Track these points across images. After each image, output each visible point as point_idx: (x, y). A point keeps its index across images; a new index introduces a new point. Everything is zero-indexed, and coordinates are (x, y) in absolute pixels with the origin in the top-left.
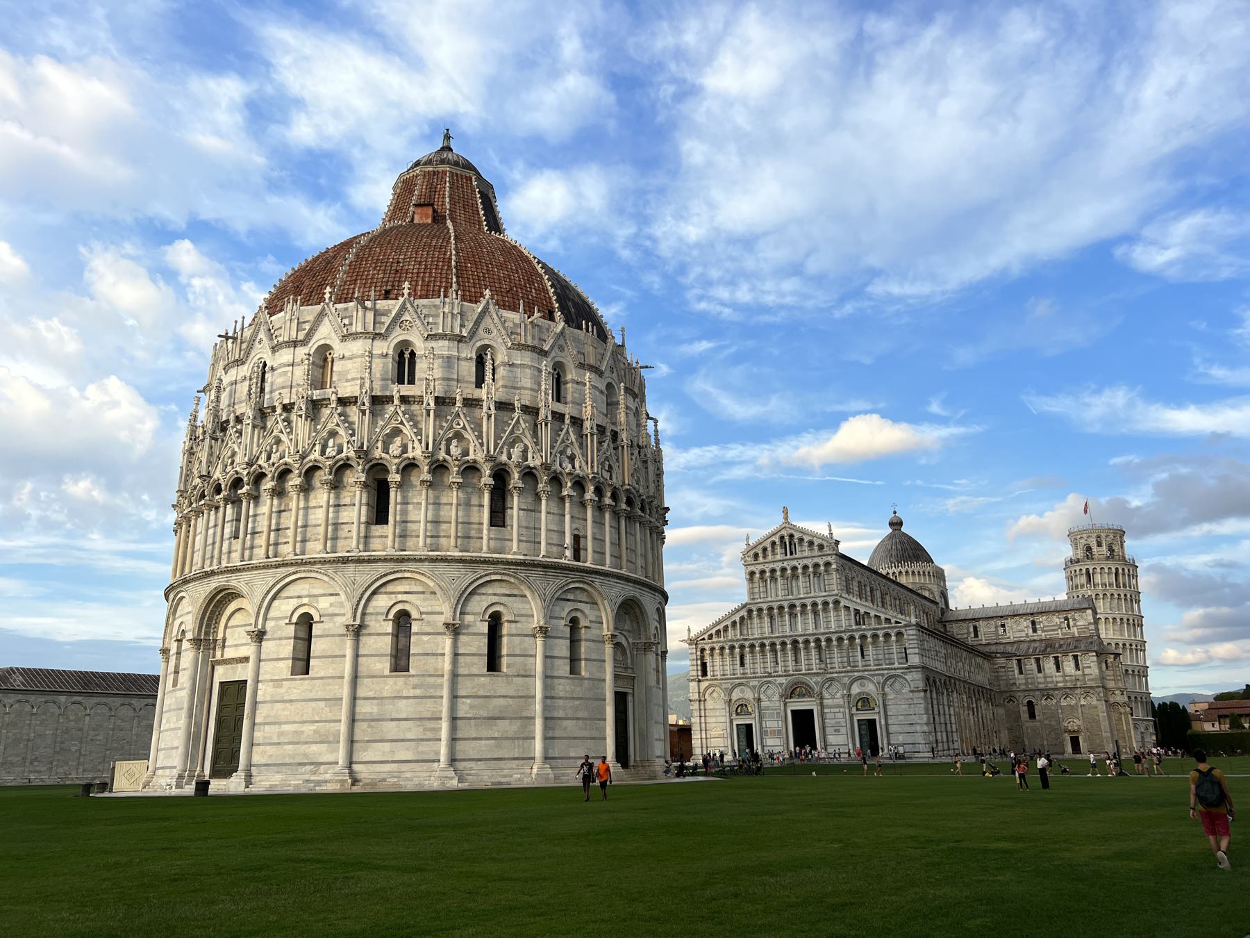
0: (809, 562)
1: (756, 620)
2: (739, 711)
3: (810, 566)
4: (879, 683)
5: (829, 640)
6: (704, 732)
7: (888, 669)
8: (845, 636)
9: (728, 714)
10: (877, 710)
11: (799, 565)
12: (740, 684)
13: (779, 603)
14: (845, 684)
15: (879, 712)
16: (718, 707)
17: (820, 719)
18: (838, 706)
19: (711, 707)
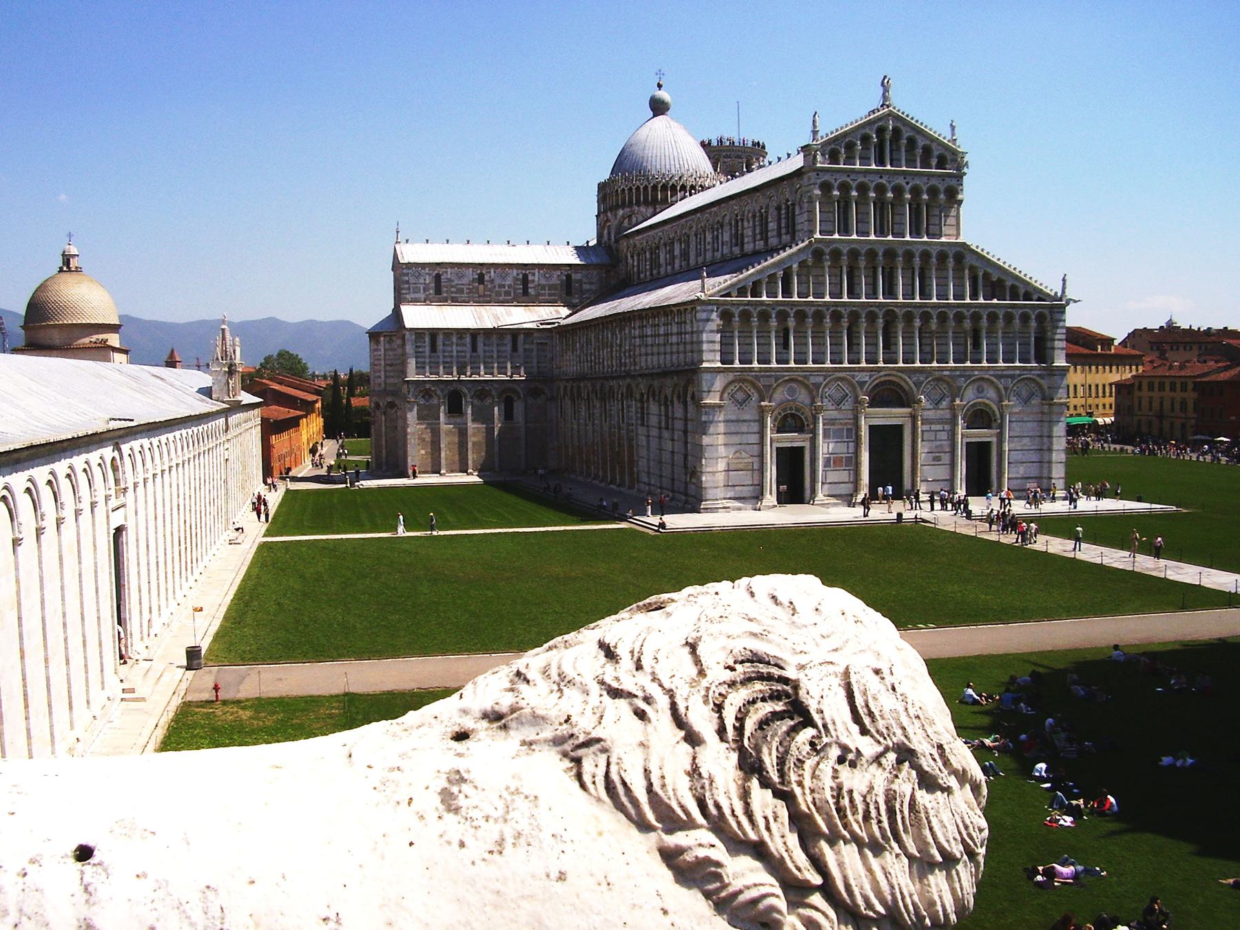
3: (925, 189)
4: (1006, 389)
12: (791, 380)
16: (747, 417)
18: (940, 421)
19: (733, 417)
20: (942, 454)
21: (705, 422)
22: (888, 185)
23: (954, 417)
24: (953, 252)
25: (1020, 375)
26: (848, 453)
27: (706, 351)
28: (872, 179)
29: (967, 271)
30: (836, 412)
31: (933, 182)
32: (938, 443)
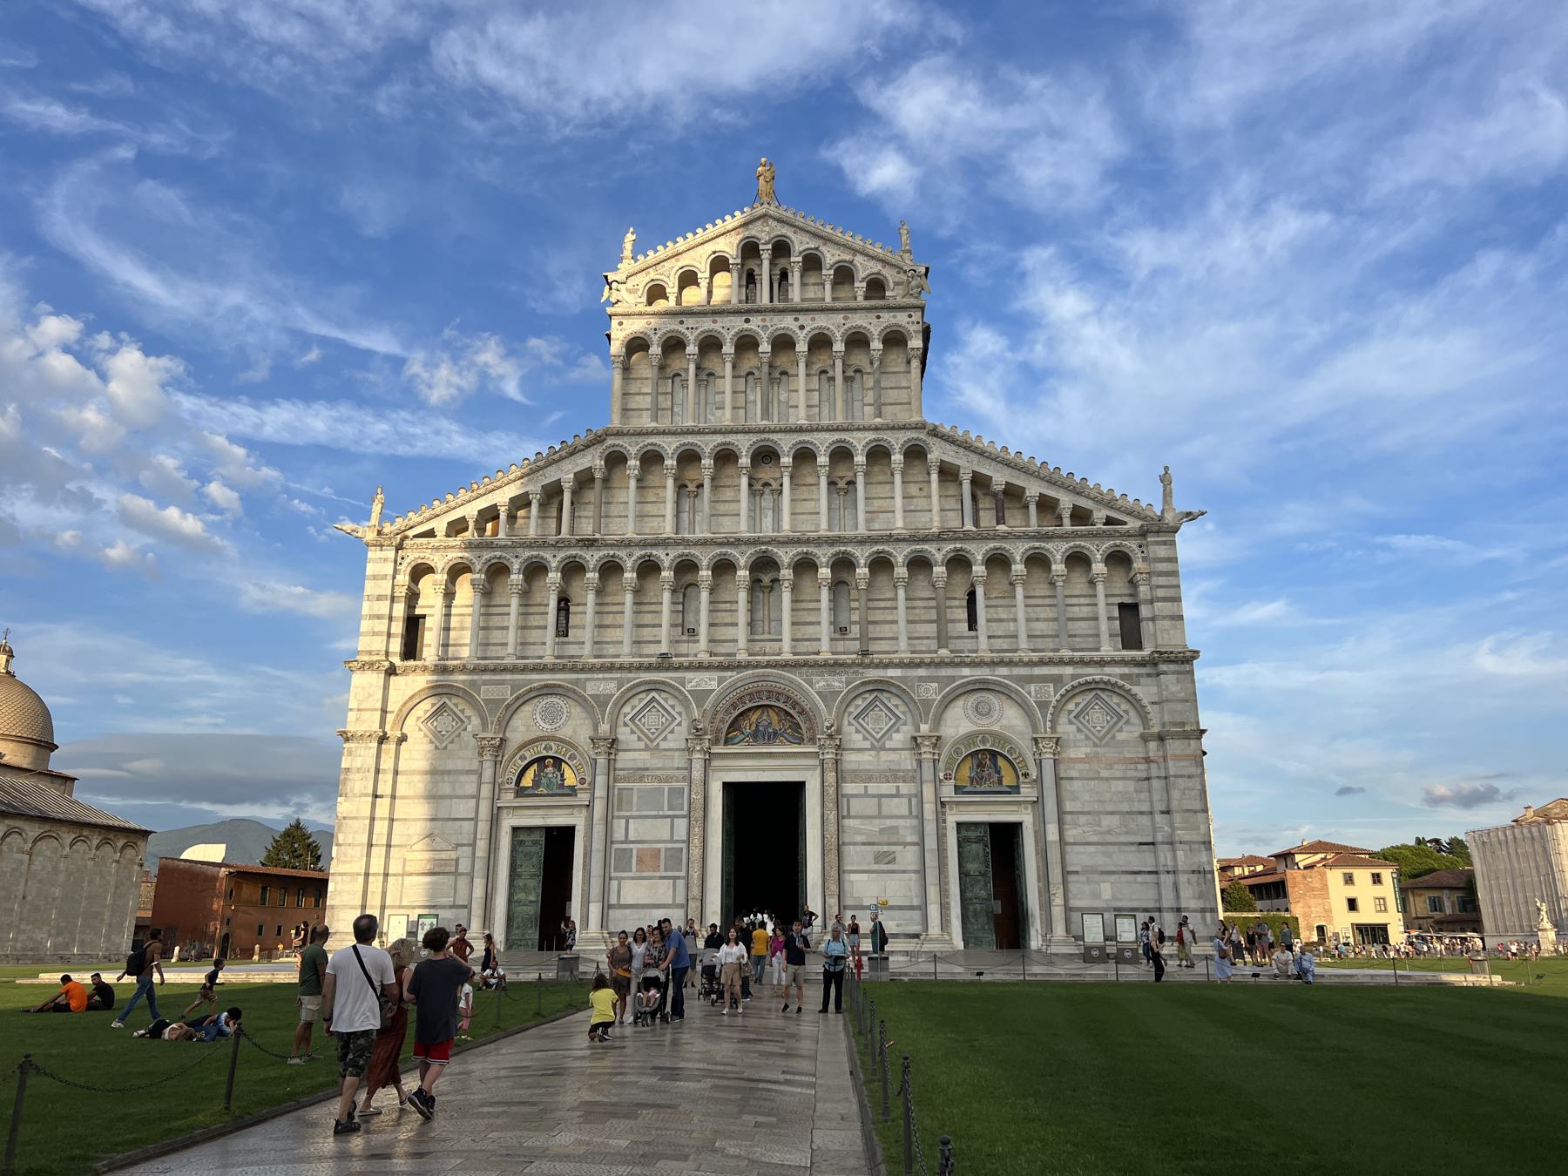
0: (836, 326)
1: (627, 493)
2: (527, 781)
3: (838, 335)
5: (881, 564)
6: (378, 853)
7: (1083, 662)
8: (938, 553)
9: (486, 790)
10: (1028, 793)
11: (801, 330)
12: (548, 690)
13: (719, 439)
14: (927, 703)
15: (1038, 803)
17: (832, 816)
18: (893, 775)
20: (899, 848)
21: (348, 770)
22: (761, 332)
23: (920, 762)
24: (901, 442)
25: (1074, 677)
26: (672, 841)
27: (366, 634)
28: (728, 325)
29: (934, 477)
30: (645, 755)
31: (858, 321)
32: (888, 823)
